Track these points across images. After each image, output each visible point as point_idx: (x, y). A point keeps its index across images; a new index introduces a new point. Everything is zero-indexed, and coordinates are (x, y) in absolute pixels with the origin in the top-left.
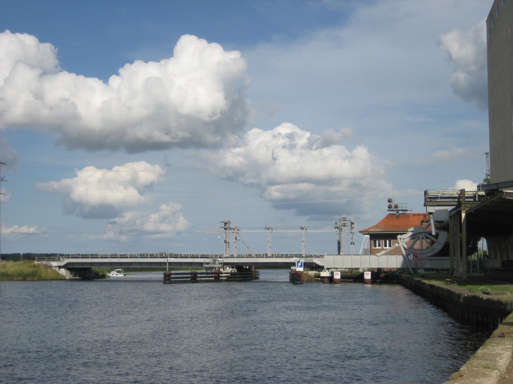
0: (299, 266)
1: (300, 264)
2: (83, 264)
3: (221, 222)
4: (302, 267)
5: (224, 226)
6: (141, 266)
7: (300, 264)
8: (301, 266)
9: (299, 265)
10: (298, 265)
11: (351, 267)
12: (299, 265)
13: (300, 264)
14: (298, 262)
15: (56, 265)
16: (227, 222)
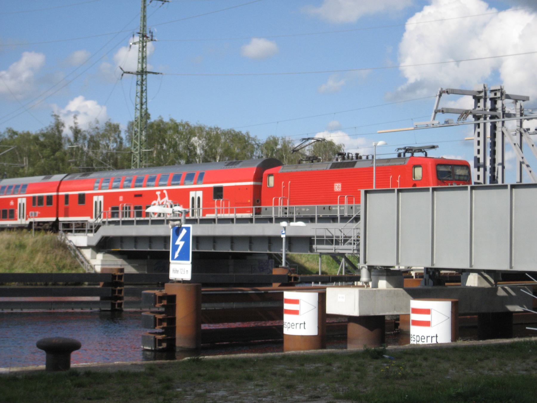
0: (176, 255)
1: (180, 243)
2: (233, 239)
3: (444, 92)
4: (189, 260)
5: (474, 108)
6: (136, 248)
7: (182, 240)
8: (183, 257)
9: (178, 246)
10: (176, 247)
11: (504, 267)
12: (178, 246)
13: (183, 243)
14: (177, 231)
15: (85, 244)
16: (480, 92)
